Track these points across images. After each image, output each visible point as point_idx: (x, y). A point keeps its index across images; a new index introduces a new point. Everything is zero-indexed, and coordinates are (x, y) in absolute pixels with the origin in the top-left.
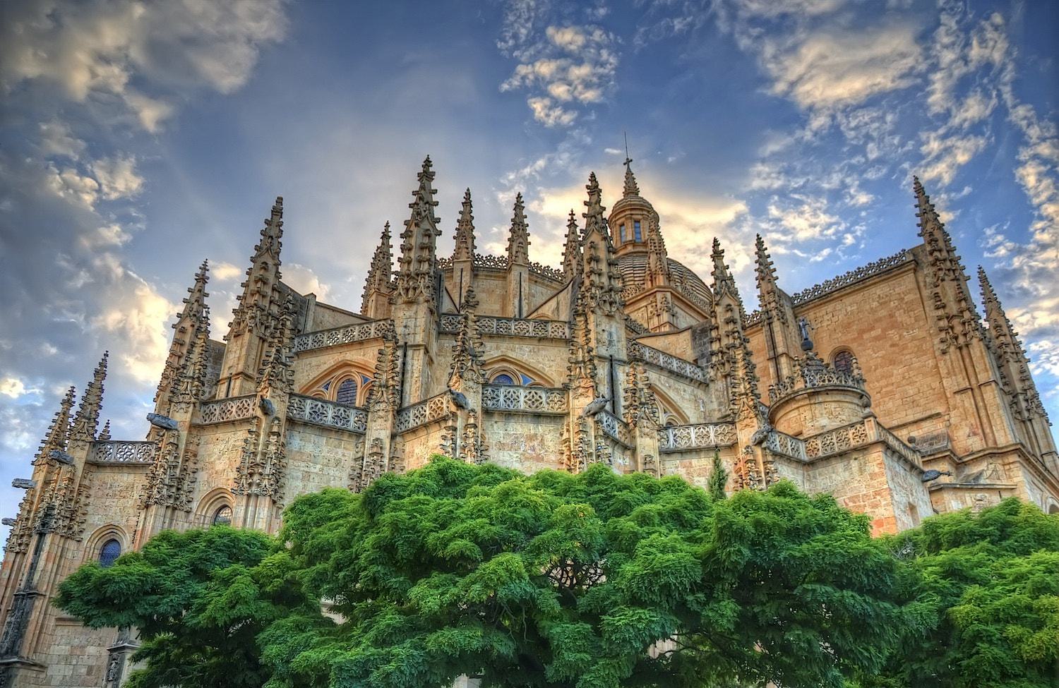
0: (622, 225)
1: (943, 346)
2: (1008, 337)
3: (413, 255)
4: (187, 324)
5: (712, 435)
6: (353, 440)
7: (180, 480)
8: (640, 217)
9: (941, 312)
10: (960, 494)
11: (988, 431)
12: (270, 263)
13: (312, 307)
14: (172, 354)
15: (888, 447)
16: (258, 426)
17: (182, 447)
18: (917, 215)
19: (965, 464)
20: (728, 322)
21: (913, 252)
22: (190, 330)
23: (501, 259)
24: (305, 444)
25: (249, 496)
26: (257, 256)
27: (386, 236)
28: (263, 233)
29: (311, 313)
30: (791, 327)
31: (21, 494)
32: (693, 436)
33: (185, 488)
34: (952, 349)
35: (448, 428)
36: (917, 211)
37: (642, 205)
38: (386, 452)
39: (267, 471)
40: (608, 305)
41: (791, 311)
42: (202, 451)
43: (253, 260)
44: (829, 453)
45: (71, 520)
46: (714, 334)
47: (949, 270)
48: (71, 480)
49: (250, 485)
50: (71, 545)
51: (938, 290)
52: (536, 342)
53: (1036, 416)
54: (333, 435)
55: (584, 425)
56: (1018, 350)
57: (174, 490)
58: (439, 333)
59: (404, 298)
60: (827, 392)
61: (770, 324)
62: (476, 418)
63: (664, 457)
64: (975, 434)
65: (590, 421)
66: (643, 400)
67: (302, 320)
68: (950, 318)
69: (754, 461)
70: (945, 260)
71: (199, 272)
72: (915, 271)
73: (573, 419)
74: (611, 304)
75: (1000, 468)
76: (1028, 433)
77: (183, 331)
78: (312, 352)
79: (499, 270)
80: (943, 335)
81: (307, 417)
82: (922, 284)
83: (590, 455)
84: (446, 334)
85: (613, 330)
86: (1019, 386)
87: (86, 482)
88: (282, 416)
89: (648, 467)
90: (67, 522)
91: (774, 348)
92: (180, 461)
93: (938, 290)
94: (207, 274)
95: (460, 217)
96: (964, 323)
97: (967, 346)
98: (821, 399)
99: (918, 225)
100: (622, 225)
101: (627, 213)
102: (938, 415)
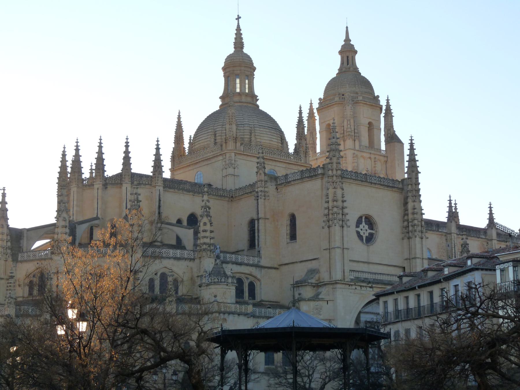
0: (228, 77)
1: (323, 224)
2: (414, 186)
8: (239, 72)
9: (326, 205)
10: (308, 302)
12: (4, 224)
13: (25, 235)
19: (320, 286)
27: (64, 155)
29: (25, 238)
41: (275, 187)
53: (414, 236)
61: (258, 200)
64: (327, 271)
67: (22, 241)
72: (322, 178)
78: (26, 261)
80: (325, 219)
86: (410, 216)
91: (258, 214)
98: (210, 287)
100: (228, 77)
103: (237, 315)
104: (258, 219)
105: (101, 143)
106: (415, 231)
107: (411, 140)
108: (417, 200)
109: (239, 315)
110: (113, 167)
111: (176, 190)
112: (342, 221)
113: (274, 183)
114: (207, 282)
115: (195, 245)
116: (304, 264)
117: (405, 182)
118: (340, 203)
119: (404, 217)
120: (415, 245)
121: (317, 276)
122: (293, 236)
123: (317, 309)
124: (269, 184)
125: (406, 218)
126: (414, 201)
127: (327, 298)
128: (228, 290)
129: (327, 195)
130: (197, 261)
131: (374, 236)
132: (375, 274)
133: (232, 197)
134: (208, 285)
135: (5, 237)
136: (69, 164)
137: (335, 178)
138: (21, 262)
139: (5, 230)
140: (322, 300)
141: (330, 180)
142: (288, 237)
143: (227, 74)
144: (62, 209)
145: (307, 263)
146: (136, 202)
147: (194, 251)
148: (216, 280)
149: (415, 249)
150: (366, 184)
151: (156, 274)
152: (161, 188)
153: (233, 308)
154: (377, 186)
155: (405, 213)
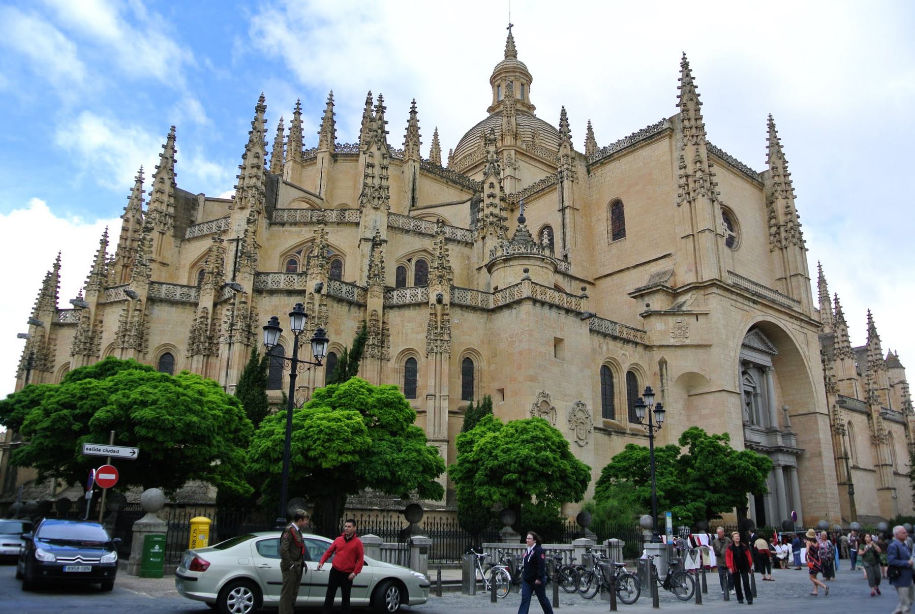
1: (679, 200)
2: (782, 177)
3: (247, 173)
4: (130, 215)
5: (420, 295)
6: (193, 309)
7: (92, 338)
8: (513, 78)
9: (682, 172)
10: (664, 318)
11: (699, 269)
12: (166, 177)
13: (201, 203)
14: (121, 238)
15: (535, 301)
16: (128, 306)
17: (92, 318)
18: (679, 88)
20: (489, 196)
21: (671, 120)
22: (132, 219)
23: (356, 146)
24: (162, 312)
25: (122, 349)
26: (158, 173)
28: (161, 155)
29: (201, 208)
30: (580, 183)
31: (23, 342)
32: (408, 296)
33: (96, 341)
34: (685, 204)
35: (231, 304)
36: (680, 84)
37: (515, 68)
38: (210, 316)
39: (133, 334)
40: (376, 200)
41: (585, 169)
42: (105, 319)
43: (154, 176)
44: (504, 303)
45: (46, 360)
46: (481, 205)
47: (693, 136)
48: (43, 336)
49: (123, 342)
50: (47, 375)
51: (683, 153)
52: (336, 226)
53: (791, 244)
54: (180, 306)
55: (312, 298)
56: (788, 188)
57: (88, 345)
58: (271, 224)
59: (238, 205)
60: (515, 258)
61: (562, 182)
62: (246, 297)
63: (388, 310)
64: (691, 271)
65: (317, 296)
66: (376, 272)
68: (687, 176)
69: (436, 315)
70: (691, 128)
71: (137, 175)
72: (671, 137)
73: (307, 293)
74: (379, 198)
75: (702, 297)
76: (783, 258)
77: (127, 221)
79: (352, 155)
80: (681, 191)
81: (163, 296)
82: (674, 147)
83: (313, 317)
84: (275, 224)
85: (378, 218)
86: (782, 219)
87: (53, 336)
88: (144, 299)
89: (374, 318)
90: (43, 362)
91: (563, 201)
92: (91, 327)
93: (683, 153)
94: (143, 176)
95: (323, 115)
96: (695, 181)
97: (694, 200)
98: (511, 263)
99: (678, 97)
100: (499, 86)
101: (503, 75)
102: (669, 255)
103: (563, 312)
104: (563, 210)
105: (331, 99)
106: (793, 237)
107: (771, 120)
108: (790, 197)
109: (568, 311)
110: (349, 133)
111: (438, 177)
112: (712, 193)
113: (584, 164)
114: (505, 254)
115: (475, 221)
116: (641, 269)
117: (766, 175)
118: (705, 166)
119: (769, 221)
120: (795, 256)
121: (672, 279)
122: (618, 232)
123: (679, 329)
124: (577, 162)
125: (773, 221)
126: (786, 198)
127: (697, 310)
128: (544, 270)
129: (682, 158)
130: (478, 245)
131: (736, 240)
132: (756, 284)
133: (513, 203)
134: (507, 260)
135: (165, 198)
136: (286, 132)
137: (694, 130)
138: (189, 240)
139: (167, 188)
140: (689, 314)
141: (688, 133)
142: (610, 235)
143: (497, 83)
144: (255, 140)
145: (647, 267)
146: (379, 131)
147: (471, 231)
148: (523, 250)
149: (796, 261)
150: (723, 162)
151: (409, 260)
152: (417, 165)
153: (557, 299)
154: (735, 170)
155: (772, 215)
